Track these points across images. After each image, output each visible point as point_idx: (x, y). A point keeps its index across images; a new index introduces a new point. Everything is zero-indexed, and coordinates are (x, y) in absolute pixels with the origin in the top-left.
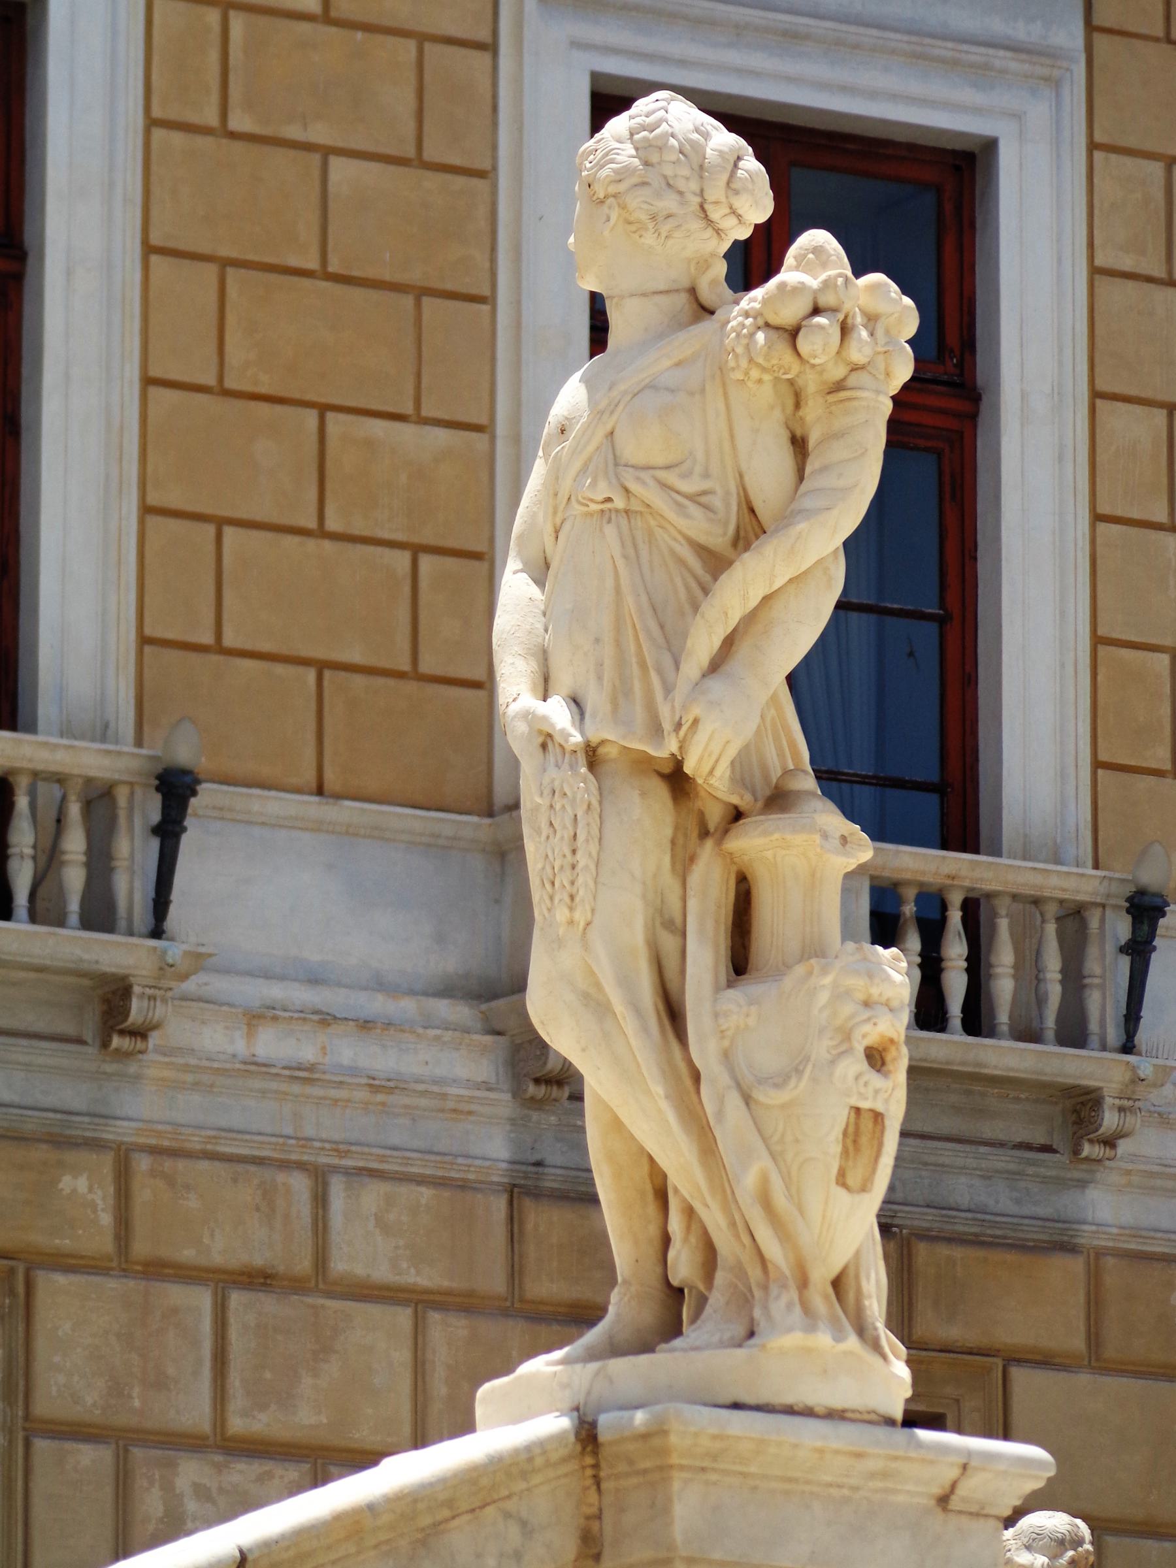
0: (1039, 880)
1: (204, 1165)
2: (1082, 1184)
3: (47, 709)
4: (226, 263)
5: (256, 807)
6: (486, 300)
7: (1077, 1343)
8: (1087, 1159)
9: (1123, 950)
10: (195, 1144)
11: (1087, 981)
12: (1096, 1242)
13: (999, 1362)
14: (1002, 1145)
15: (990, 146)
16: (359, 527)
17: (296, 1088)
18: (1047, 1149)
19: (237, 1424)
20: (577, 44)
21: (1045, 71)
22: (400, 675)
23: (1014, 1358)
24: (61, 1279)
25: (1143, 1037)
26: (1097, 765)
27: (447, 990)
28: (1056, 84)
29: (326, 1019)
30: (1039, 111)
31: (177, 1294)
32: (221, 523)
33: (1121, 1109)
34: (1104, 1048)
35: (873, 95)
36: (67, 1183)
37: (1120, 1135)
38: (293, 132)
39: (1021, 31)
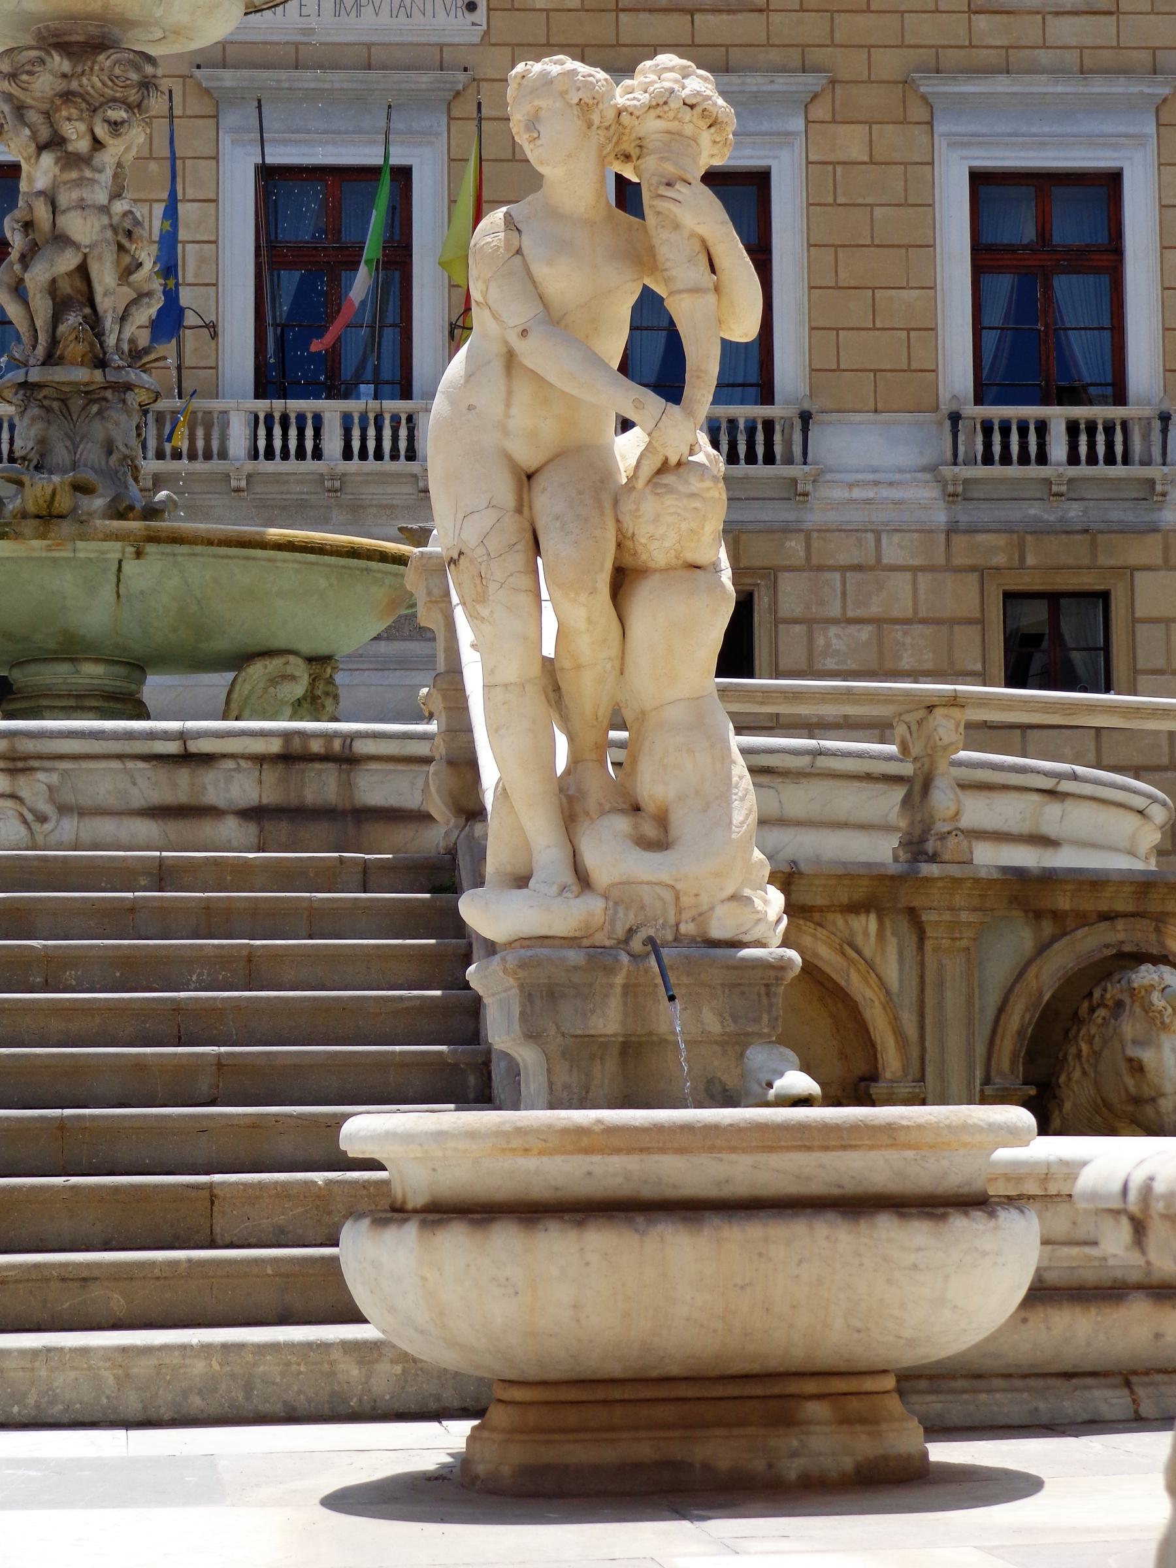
0: (1127, 412)
1: (837, 534)
2: (1160, 509)
3: (778, 396)
4: (836, 246)
5: (852, 419)
6: (933, 246)
7: (1160, 561)
10: (834, 527)
14: (1127, 499)
16: (888, 324)
17: (867, 506)
19: (850, 614)
20: (962, 158)
22: (905, 371)
23: (1134, 569)
24: (786, 574)
25: (1169, 459)
26: (1166, 370)
27: (924, 469)
29: (876, 483)
31: (828, 575)
32: (837, 330)
34: (1156, 465)
35: (1075, 159)
36: (787, 544)
38: (861, 201)
39: (1131, 130)
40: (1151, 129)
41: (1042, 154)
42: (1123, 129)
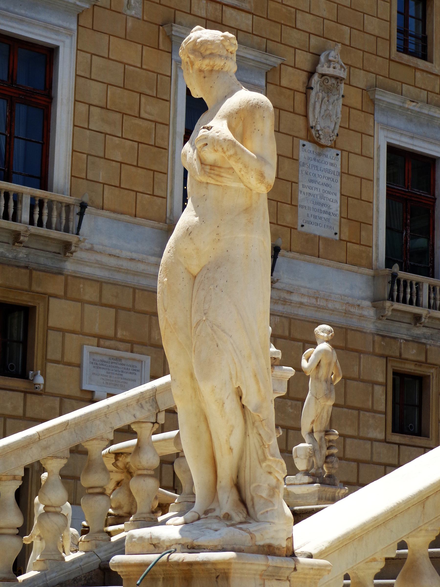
0: (62, 198)
2: (65, 261)
7: (62, 293)
8: (67, 256)
9: (77, 214)
11: (70, 220)
12: (67, 273)
13: (47, 296)
14: (51, 252)
15: (57, 48)
18: (59, 253)
21: (69, 33)
23: (51, 296)
28: (71, 36)
30: (68, 41)
33: (75, 246)
34: (73, 233)
35: (36, 34)
37: (75, 252)
40: (74, 26)
41: (20, 27)
42: (61, 23)
